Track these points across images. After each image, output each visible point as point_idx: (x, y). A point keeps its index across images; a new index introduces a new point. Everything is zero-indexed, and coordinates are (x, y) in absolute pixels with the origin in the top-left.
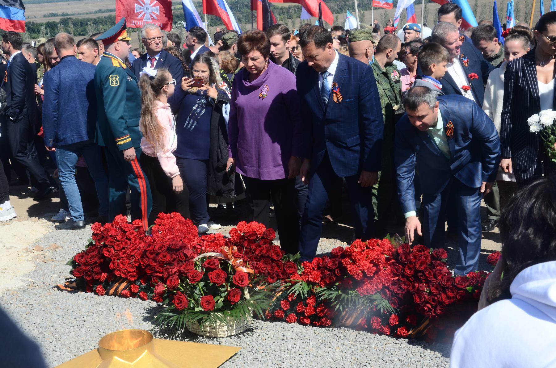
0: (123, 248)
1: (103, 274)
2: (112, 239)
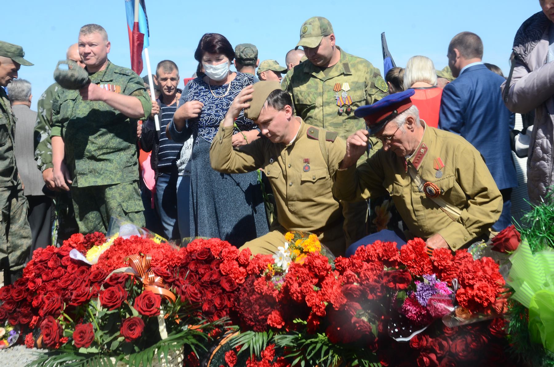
0: (55, 278)
1: (34, 317)
2: (41, 265)
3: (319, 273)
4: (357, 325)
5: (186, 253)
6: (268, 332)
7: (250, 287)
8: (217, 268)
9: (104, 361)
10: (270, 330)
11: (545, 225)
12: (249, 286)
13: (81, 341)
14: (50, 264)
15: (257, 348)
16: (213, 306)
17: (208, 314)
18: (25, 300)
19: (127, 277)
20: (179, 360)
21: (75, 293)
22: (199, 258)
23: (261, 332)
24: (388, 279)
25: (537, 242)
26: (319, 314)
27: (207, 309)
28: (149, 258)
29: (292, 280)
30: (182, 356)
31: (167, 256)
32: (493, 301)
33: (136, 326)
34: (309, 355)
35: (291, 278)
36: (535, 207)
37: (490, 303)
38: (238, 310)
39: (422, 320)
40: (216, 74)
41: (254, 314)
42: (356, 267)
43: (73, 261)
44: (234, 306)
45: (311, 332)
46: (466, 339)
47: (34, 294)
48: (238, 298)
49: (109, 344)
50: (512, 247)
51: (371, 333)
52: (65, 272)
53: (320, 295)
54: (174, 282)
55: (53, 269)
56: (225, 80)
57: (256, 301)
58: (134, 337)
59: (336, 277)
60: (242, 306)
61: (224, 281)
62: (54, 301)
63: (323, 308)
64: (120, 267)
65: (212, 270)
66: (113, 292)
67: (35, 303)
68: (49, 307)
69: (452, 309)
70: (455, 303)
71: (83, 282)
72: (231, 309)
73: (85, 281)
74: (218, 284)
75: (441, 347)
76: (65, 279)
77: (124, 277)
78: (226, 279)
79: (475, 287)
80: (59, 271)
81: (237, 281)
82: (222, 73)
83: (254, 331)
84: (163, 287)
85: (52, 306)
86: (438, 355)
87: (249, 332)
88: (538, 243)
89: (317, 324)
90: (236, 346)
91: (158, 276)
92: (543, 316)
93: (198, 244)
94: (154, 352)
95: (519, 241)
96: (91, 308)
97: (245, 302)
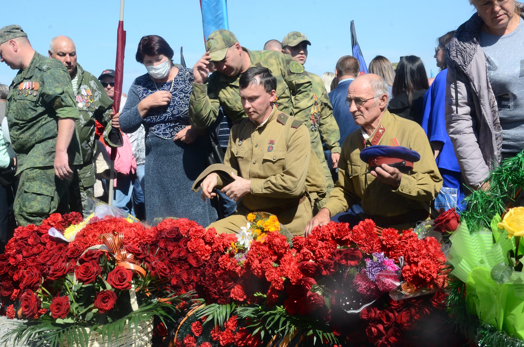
2: (22, 242)
3: (278, 250)
4: (312, 298)
5: (157, 232)
6: (231, 305)
7: (215, 263)
8: (185, 246)
9: (79, 331)
10: (233, 303)
11: (482, 208)
12: (214, 262)
13: (57, 312)
14: (30, 241)
15: (221, 319)
16: (181, 280)
17: (176, 288)
18: (6, 274)
19: (101, 253)
20: (149, 330)
21: (52, 268)
22: (168, 236)
23: (224, 304)
24: (340, 256)
25: (475, 223)
26: (278, 288)
27: (175, 283)
28: (121, 236)
29: (254, 257)
30: (152, 327)
31: (138, 234)
32: (435, 277)
33: (109, 298)
34: (268, 325)
35: (252, 255)
36: (473, 191)
37: (433, 279)
38: (203, 284)
39: (371, 294)
40: (158, 74)
41: (218, 288)
42: (311, 245)
43: (52, 239)
44: (200, 280)
45: (270, 305)
46: (411, 311)
47: (15, 268)
48: (204, 273)
49: (84, 315)
50: (452, 227)
51: (325, 306)
52: (44, 249)
53: (278, 271)
54: (145, 258)
55: (33, 246)
56: (167, 78)
57: (220, 276)
58: (107, 308)
59: (294, 255)
60: (207, 281)
61: (192, 257)
62: (33, 275)
63: (281, 283)
64: (95, 245)
65: (180, 247)
66: (88, 267)
67: (16, 277)
68: (28, 281)
69: (398, 284)
70: (401, 279)
71: (60, 258)
72: (197, 283)
73: (62, 257)
74: (186, 260)
75: (388, 318)
76: (44, 255)
77: (98, 253)
78: (193, 255)
79: (419, 264)
80: (39, 248)
81: (203, 258)
82: (163, 71)
83: (218, 304)
84: (134, 263)
85: (31, 280)
86: (385, 326)
87: (214, 304)
88: (475, 225)
89: (276, 298)
90: (201, 317)
91: (130, 253)
92: (479, 290)
93: (168, 223)
94: (125, 322)
95: (459, 222)
96: (67, 282)
97: (210, 277)
